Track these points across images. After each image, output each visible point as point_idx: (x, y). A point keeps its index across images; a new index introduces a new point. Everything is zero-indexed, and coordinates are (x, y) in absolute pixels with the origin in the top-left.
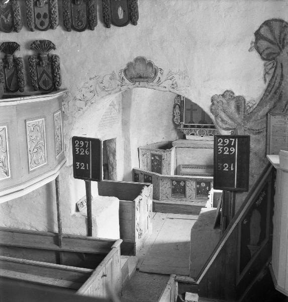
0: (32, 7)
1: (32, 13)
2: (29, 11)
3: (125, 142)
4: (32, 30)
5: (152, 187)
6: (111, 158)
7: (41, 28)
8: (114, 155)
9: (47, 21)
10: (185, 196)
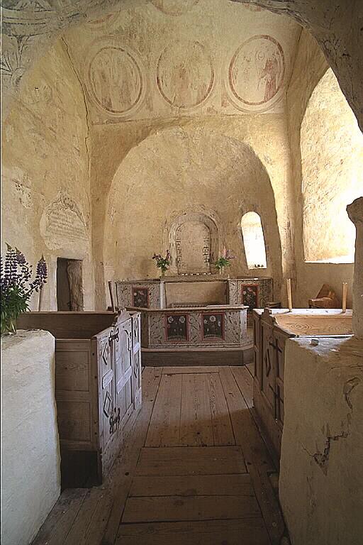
3: (96, 270)
5: (139, 318)
6: (76, 292)
8: (80, 286)
10: (187, 339)
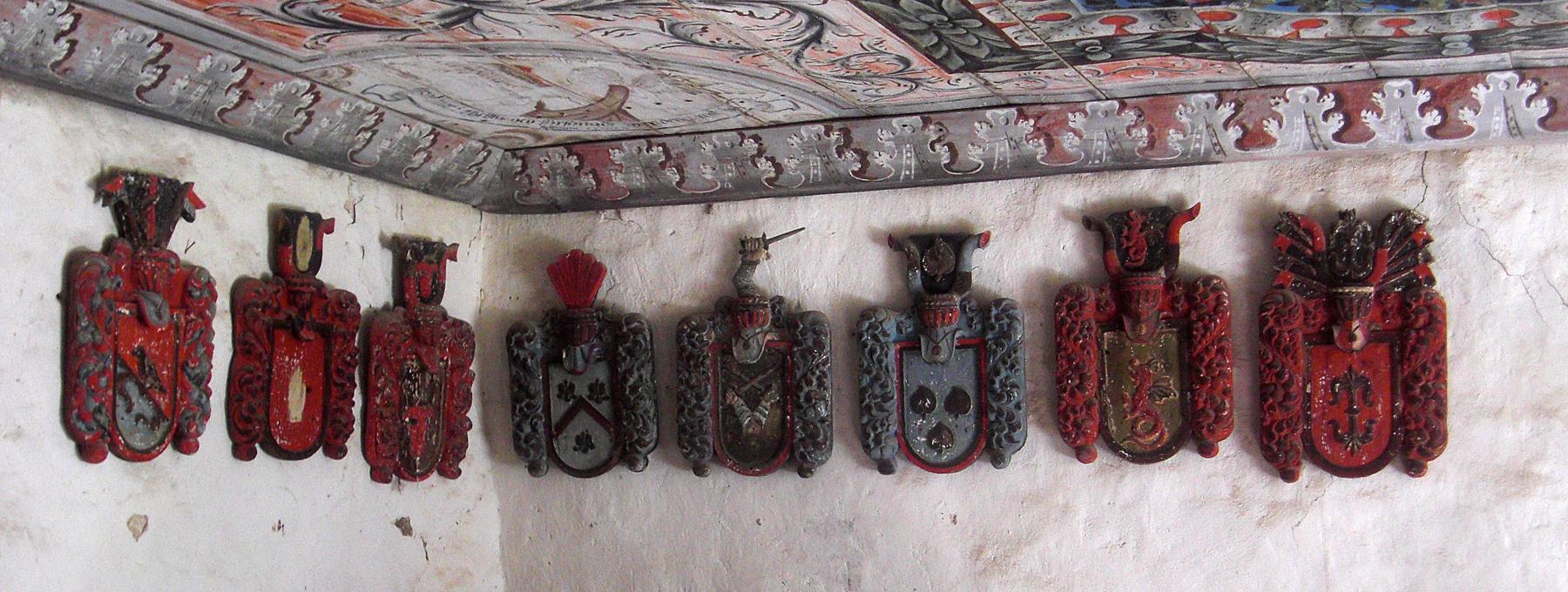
0: (891, 359)
1: (892, 388)
2: (877, 378)
4: (885, 468)
7: (932, 456)
9: (964, 427)
